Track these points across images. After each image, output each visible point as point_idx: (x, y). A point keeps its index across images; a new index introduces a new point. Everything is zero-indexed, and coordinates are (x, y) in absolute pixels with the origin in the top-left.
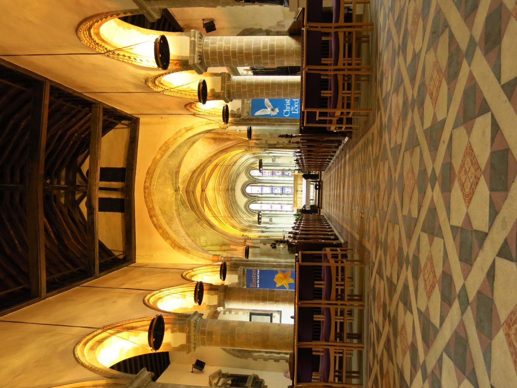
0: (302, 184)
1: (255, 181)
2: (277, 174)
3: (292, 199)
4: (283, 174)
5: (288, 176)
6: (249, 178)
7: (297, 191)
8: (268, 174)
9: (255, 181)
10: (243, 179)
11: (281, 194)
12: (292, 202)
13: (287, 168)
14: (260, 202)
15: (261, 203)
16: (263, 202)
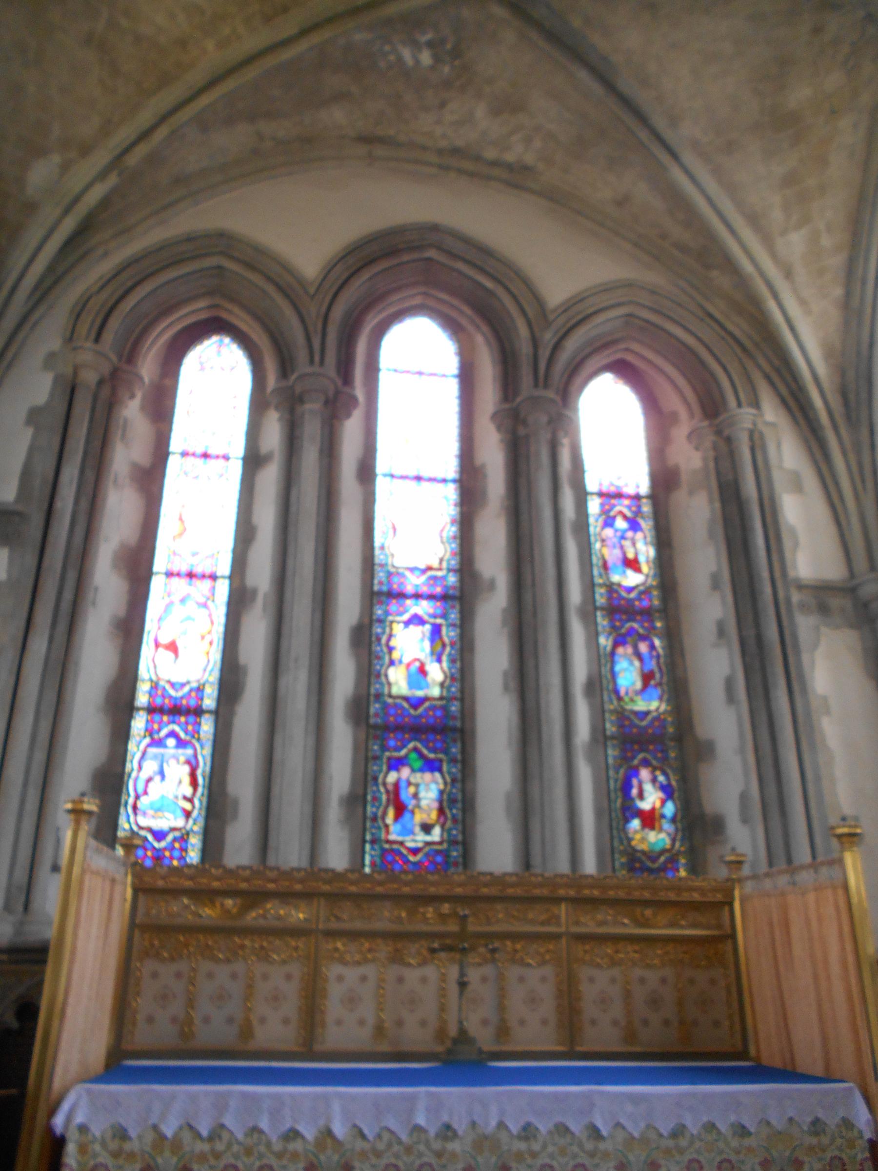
0: (573, 1050)
1: (542, 380)
2: (628, 675)
3: (291, 854)
4: (634, 742)
5: (620, 805)
6: (578, 313)
7: (455, 945)
8: (612, 555)
9: (542, 380)
10: (562, 267)
11: (358, 710)
12: (240, 849)
13: (729, 782)
14: (273, 436)
15: (253, 461)
16: (270, 478)
